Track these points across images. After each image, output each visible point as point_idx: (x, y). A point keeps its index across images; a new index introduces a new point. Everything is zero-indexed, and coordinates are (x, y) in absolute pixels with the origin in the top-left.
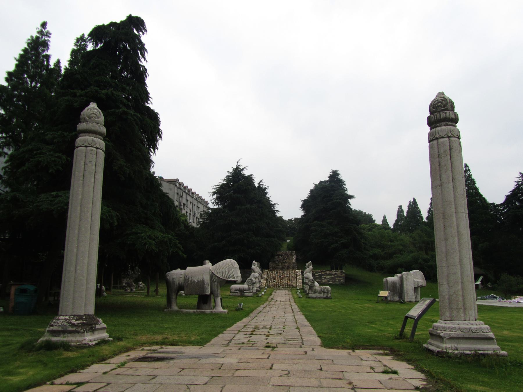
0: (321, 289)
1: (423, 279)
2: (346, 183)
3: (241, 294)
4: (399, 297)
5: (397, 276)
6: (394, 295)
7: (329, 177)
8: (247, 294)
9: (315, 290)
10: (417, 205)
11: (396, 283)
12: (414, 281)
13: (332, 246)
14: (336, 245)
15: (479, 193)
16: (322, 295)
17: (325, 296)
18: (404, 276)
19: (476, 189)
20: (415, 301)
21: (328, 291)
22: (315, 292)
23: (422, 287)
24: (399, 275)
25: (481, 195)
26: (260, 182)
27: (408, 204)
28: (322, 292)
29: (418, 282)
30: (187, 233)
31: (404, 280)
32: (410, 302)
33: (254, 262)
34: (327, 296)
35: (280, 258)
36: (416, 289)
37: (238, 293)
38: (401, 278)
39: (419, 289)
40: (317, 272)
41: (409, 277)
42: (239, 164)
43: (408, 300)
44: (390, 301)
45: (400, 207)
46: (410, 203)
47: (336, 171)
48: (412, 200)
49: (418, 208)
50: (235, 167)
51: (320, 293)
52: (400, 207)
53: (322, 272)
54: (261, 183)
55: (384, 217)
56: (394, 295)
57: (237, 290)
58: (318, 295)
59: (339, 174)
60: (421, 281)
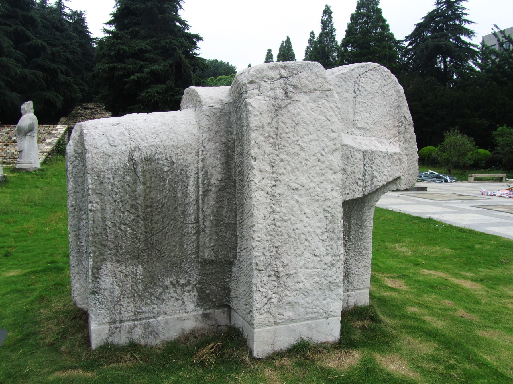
4: (203, 299)
5: (197, 103)
10: (291, 47)
11: (179, 174)
12: (347, 154)
13: (132, 77)
14: (139, 75)
15: (382, 17)
19: (379, 11)
25: (385, 21)
27: (279, 46)
29: (368, 156)
35: (88, 112)
43: (285, 341)
45: (270, 51)
46: (282, 44)
48: (285, 39)
49: (292, 50)
52: (270, 51)
56: (149, 288)
60: (394, 148)
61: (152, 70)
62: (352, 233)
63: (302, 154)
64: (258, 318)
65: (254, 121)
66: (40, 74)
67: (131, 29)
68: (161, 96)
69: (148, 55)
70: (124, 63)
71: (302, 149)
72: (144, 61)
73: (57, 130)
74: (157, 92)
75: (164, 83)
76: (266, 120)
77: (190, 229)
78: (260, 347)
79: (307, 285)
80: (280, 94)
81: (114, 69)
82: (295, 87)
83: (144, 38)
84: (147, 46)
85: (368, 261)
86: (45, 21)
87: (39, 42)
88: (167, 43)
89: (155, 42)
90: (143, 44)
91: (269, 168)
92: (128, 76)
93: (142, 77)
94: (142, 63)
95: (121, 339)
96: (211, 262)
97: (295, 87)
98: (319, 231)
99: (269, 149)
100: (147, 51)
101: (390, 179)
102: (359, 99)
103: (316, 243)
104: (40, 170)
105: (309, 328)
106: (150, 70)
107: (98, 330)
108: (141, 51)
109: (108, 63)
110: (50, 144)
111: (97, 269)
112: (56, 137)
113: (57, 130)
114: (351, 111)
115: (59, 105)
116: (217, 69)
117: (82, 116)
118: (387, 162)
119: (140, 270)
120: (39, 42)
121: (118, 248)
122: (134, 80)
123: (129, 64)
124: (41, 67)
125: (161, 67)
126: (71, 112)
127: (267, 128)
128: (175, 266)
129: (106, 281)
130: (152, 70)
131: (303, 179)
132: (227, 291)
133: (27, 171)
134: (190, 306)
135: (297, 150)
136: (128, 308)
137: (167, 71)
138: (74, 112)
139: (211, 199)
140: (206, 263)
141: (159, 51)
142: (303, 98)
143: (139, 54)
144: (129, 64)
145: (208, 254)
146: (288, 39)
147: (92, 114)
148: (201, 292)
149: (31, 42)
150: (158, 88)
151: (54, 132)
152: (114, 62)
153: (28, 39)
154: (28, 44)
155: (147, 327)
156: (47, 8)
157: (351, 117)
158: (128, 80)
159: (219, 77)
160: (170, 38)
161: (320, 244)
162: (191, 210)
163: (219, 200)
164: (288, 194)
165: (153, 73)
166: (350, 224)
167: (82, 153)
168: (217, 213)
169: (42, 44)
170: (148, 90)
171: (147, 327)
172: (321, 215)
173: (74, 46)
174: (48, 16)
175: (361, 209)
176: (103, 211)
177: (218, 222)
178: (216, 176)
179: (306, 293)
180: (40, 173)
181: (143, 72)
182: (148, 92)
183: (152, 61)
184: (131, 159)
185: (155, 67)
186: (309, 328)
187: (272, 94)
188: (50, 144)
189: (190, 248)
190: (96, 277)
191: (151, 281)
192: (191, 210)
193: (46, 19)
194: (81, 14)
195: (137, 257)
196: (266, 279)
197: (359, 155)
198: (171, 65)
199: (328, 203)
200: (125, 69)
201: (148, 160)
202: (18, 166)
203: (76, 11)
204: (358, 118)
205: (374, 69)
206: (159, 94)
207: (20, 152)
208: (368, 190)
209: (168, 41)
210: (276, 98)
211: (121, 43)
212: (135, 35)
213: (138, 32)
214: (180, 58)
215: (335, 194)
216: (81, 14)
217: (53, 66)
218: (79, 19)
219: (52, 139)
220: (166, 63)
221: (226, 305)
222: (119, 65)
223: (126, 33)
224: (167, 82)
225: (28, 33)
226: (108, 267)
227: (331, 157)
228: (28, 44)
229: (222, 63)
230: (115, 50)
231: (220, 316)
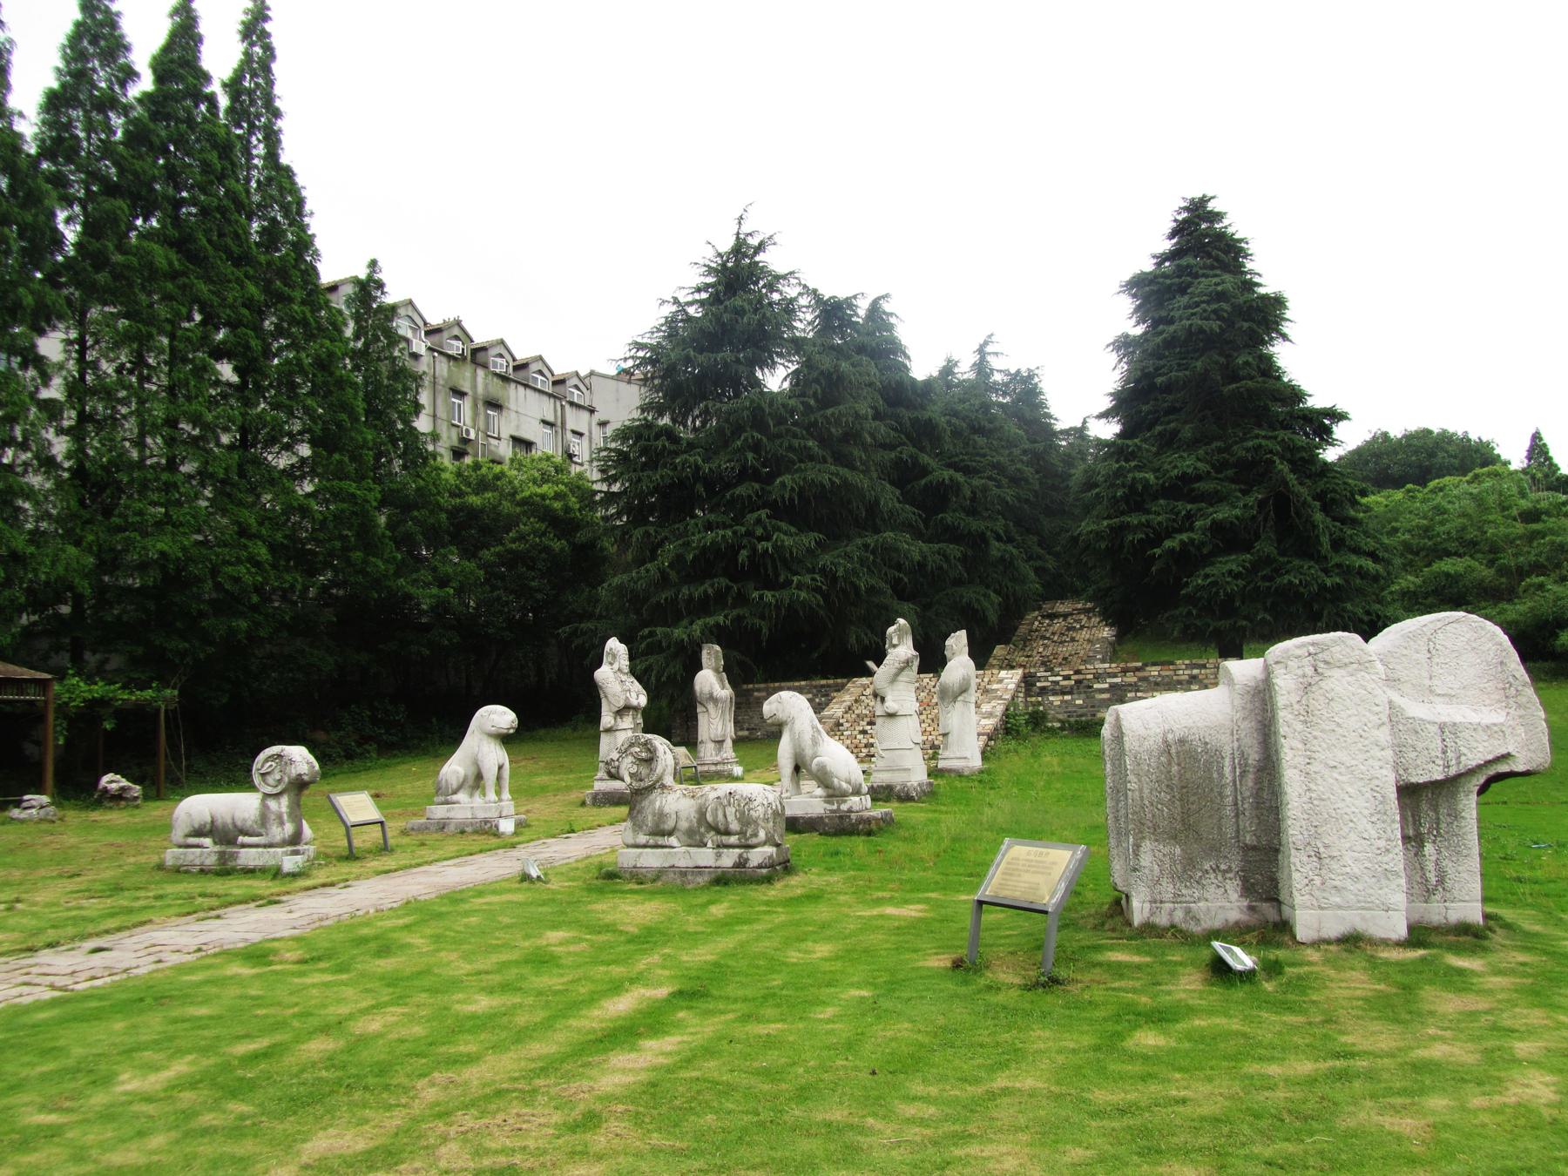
0: (702, 814)
1: (1507, 694)
2: (1252, 248)
3: (222, 854)
4: (1248, 889)
5: (1231, 682)
6: (1187, 871)
7: (1173, 235)
8: (248, 857)
9: (661, 816)
11: (1215, 755)
13: (1168, 544)
14: (1184, 537)
16: (705, 857)
17: (729, 859)
18: (1284, 684)
20: (1419, 935)
21: (746, 820)
22: (660, 832)
23: (1495, 778)
24: (1243, 670)
26: (986, 343)
28: (705, 828)
30: (557, 545)
31: (1287, 723)
32: (1352, 941)
33: (614, 644)
34: (741, 864)
35: (1059, 624)
36: (1421, 801)
37: (208, 850)
38: (1262, 698)
39: (1469, 803)
40: (1098, 677)
41: (1337, 682)
42: (745, 229)
43: (1333, 929)
44: (1149, 929)
47: (1204, 201)
50: (726, 245)
51: (695, 839)
53: (1125, 671)
54: (989, 349)
55: (1536, 437)
56: (1187, 871)
57: (198, 833)
58: (680, 855)
59: (1218, 216)
61: (1214, 522)
62: (1443, 826)
63: (1340, 731)
64: (1298, 899)
65: (1281, 701)
66: (954, 550)
67: (1159, 428)
68: (1240, 582)
69: (1202, 486)
70: (1148, 512)
71: (1339, 725)
72: (1193, 501)
73: (1001, 681)
74: (1230, 572)
75: (1248, 548)
76: (1294, 698)
77: (1229, 811)
78: (1302, 933)
79: (1356, 870)
80: (1309, 671)
81: (1124, 527)
82: (1326, 663)
83: (1193, 444)
84: (1199, 465)
85: (1474, 863)
86: (954, 420)
87: (947, 474)
88: (1248, 450)
89: (1220, 451)
90: (1187, 463)
91: (1300, 746)
92: (1157, 542)
93: (1192, 541)
94: (1189, 507)
95: (1162, 920)
96: (1254, 848)
97: (1326, 663)
98: (1366, 812)
99: (1300, 727)
100: (1199, 478)
101: (1490, 757)
102: (1435, 660)
103: (1363, 824)
104: (981, 772)
105: (1363, 918)
106: (1209, 521)
107: (1140, 910)
108: (1184, 478)
109: (1109, 517)
110: (990, 715)
111: (1137, 846)
112: (1000, 698)
113: (1001, 681)
114: (1426, 674)
115: (993, 617)
116: (1432, 455)
117: (1044, 638)
118: (1482, 736)
119: (1178, 850)
120: (947, 474)
121: (1155, 827)
122: (1172, 551)
123: (1159, 513)
124: (952, 534)
125: (1237, 512)
126: (1016, 629)
127: (1296, 707)
128: (1214, 850)
129: (1146, 859)
130: (1214, 522)
131: (1342, 756)
132: (1274, 882)
133: (959, 774)
134: (1234, 896)
135: (1333, 726)
136: (1167, 889)
137: (1254, 517)
138: (1023, 629)
139: (1250, 780)
140: (1247, 849)
141: (1230, 472)
142: (1336, 673)
143: (1181, 487)
144: (1159, 513)
145: (1249, 839)
146: (1536, 437)
147: (1069, 629)
148: (1245, 880)
149: (930, 478)
150: (1232, 563)
151: (995, 686)
152: (1123, 513)
153: (925, 471)
154: (923, 482)
155: (1188, 911)
156: (957, 386)
157: (1427, 682)
158: (1158, 551)
159: (1432, 484)
160: (1257, 437)
161: (1369, 826)
162: (1228, 791)
163: (1258, 781)
164: (1326, 772)
165: (1217, 528)
166: (1437, 813)
167: (1119, 737)
168: (1257, 795)
169: (951, 479)
170: (1208, 570)
171: (1188, 911)
172: (1368, 795)
173: (1019, 466)
174: (960, 407)
175: (1453, 795)
176: (1141, 790)
177: (1258, 804)
178: (1254, 756)
179: (1356, 879)
180: (983, 778)
181: (1191, 529)
182: (1207, 576)
183: (1215, 499)
184: (1165, 741)
185: (1223, 513)
186: (1363, 918)
187: (1300, 672)
188: (990, 715)
189: (1230, 832)
190: (1136, 855)
191: (1190, 863)
192: (1228, 791)
193: (955, 414)
194: (1031, 376)
195: (1175, 838)
196: (1305, 859)
197: (1435, 729)
198: (1262, 504)
199: (1376, 782)
200: (1148, 525)
201: (1182, 741)
202: (941, 764)
203: (1018, 371)
204: (1435, 682)
205: (1457, 621)
206: (1237, 576)
207: (945, 735)
208: (1453, 771)
209: (1250, 444)
210: (1304, 676)
211: (1138, 468)
212: (1169, 441)
213: (1175, 433)
214: (1285, 483)
215: (1384, 772)
216: (1031, 376)
217: (976, 525)
218: (1026, 392)
219: (993, 703)
220: (1250, 500)
221: (1275, 900)
222: (1133, 519)
223: (1145, 440)
224: (1257, 546)
225: (925, 459)
226: (1147, 845)
227: (1376, 732)
228: (923, 482)
229: (1445, 438)
230: (1124, 486)
231: (1268, 910)
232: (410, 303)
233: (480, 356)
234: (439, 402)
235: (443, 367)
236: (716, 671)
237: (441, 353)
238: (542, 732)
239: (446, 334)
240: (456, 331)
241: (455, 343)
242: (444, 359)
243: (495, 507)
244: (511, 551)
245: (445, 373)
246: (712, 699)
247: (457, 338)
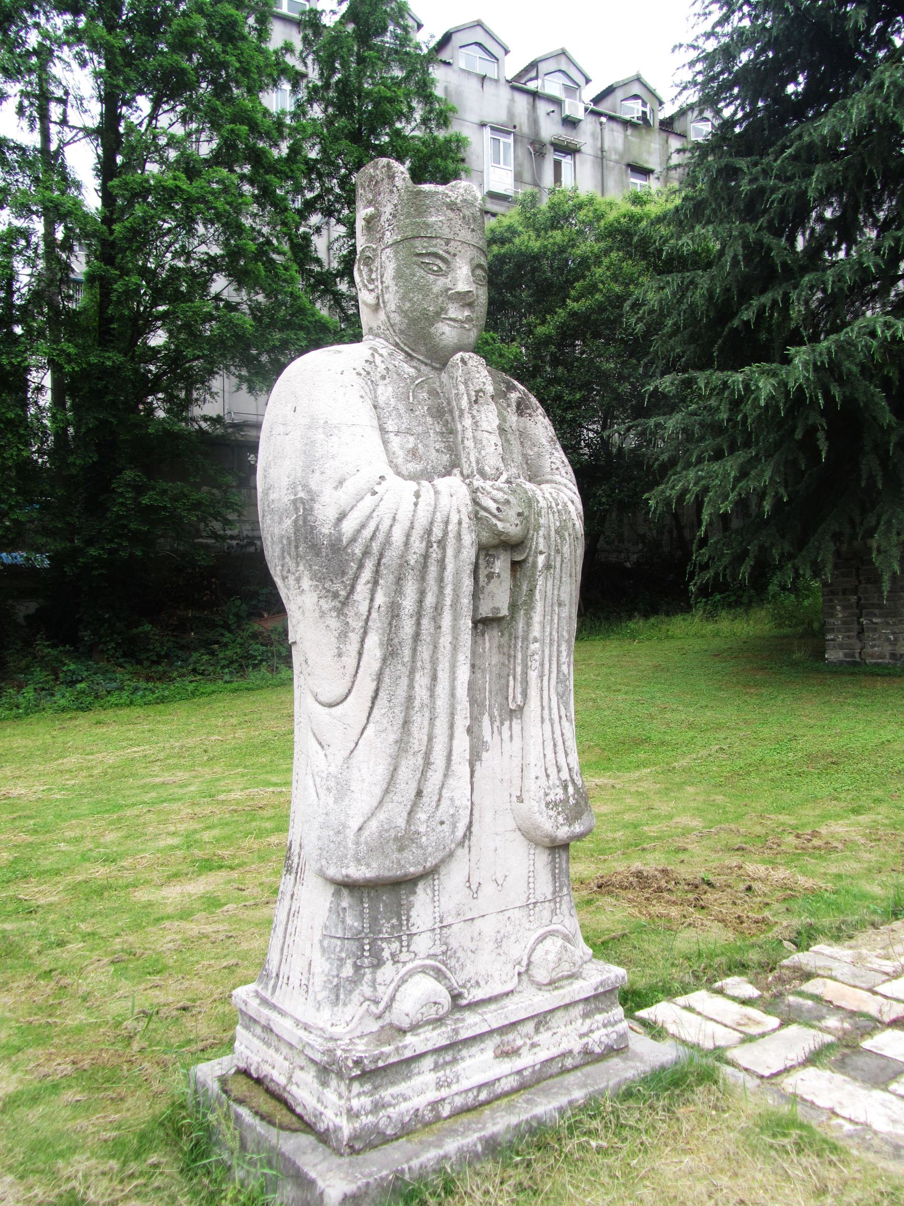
232: (564, 53)
233: (678, 127)
234: (611, 183)
235: (615, 137)
236: (418, 341)
237: (611, 118)
238: (637, 624)
239: (619, 94)
240: (636, 89)
241: (631, 104)
242: (617, 127)
243: (562, 250)
244: (573, 314)
245: (620, 144)
246: (335, 561)
247: (636, 97)
